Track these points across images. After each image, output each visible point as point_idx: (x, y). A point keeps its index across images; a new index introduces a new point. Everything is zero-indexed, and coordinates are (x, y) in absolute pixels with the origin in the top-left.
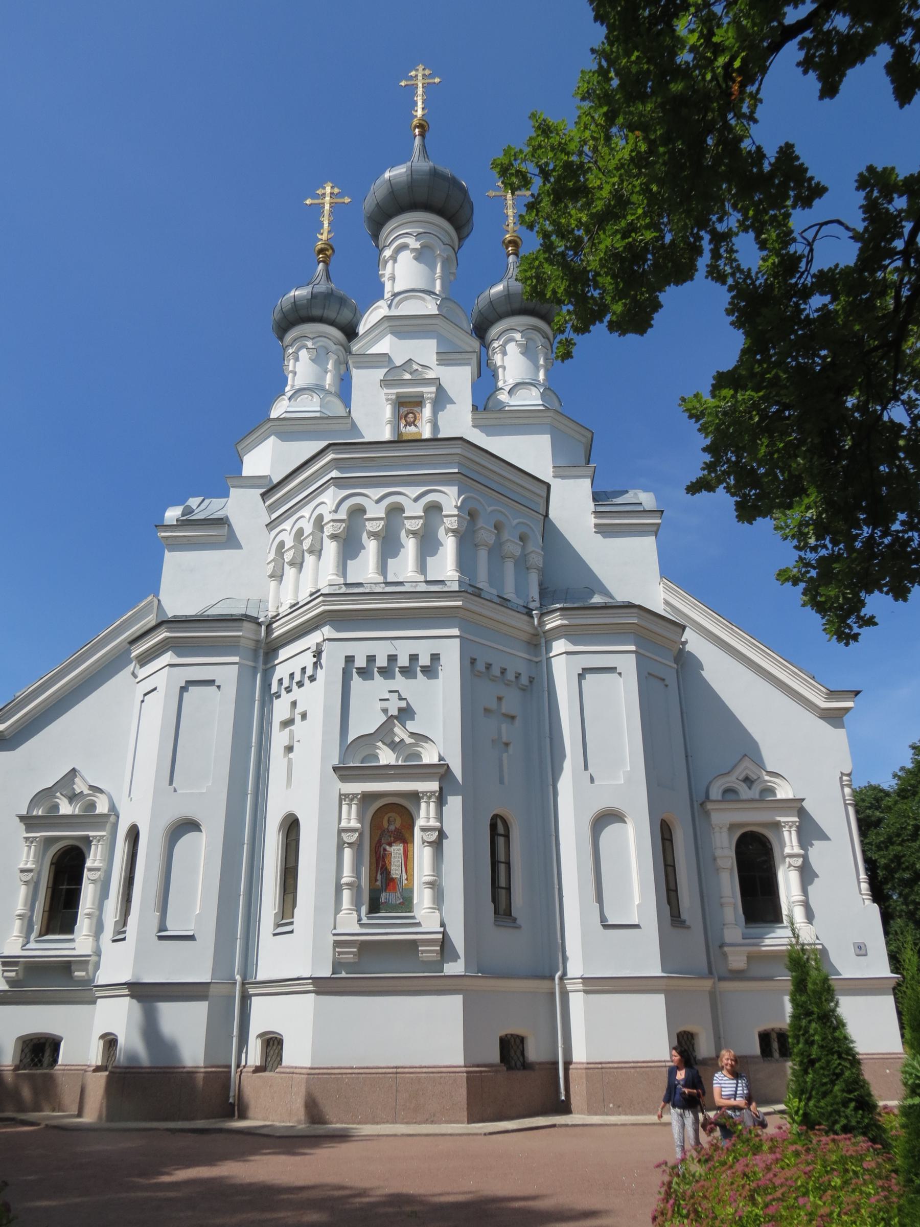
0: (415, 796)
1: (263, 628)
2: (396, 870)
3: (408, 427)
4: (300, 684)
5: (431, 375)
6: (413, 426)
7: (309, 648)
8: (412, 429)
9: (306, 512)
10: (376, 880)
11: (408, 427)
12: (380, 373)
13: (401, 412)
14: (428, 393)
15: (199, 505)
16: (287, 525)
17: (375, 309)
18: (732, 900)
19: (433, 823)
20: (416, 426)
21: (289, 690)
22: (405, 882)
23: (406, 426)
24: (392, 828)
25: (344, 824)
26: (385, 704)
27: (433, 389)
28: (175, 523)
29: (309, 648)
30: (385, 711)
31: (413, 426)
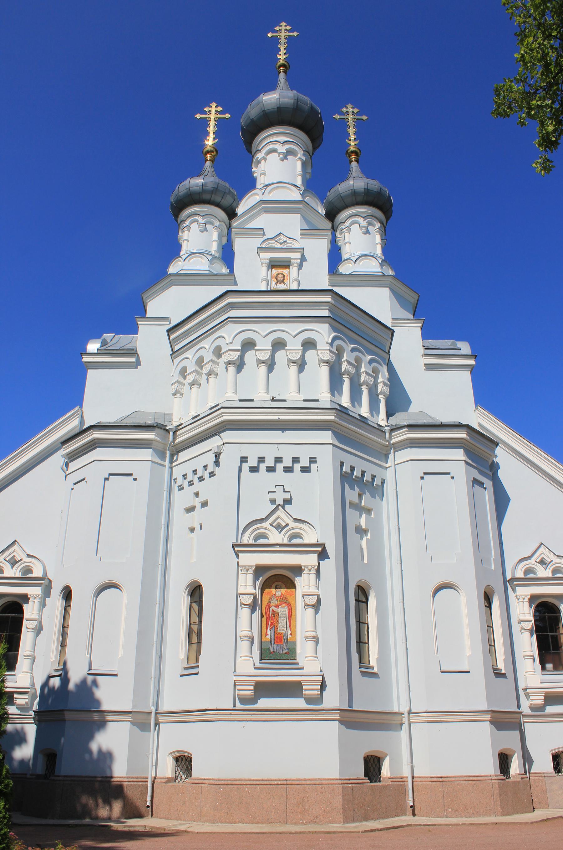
0: (298, 570)
1: (171, 433)
2: (282, 628)
3: (278, 284)
4: (201, 479)
5: (297, 245)
6: (282, 284)
7: (211, 450)
9: (207, 344)
10: (267, 635)
11: (278, 284)
12: (257, 242)
13: (273, 273)
15: (112, 340)
16: (189, 354)
17: (252, 195)
19: (313, 590)
20: (284, 283)
21: (191, 483)
22: (289, 636)
23: (276, 283)
25: (241, 590)
26: (272, 496)
27: (298, 255)
28: (96, 352)
29: (211, 450)
30: (273, 501)
31: (282, 284)
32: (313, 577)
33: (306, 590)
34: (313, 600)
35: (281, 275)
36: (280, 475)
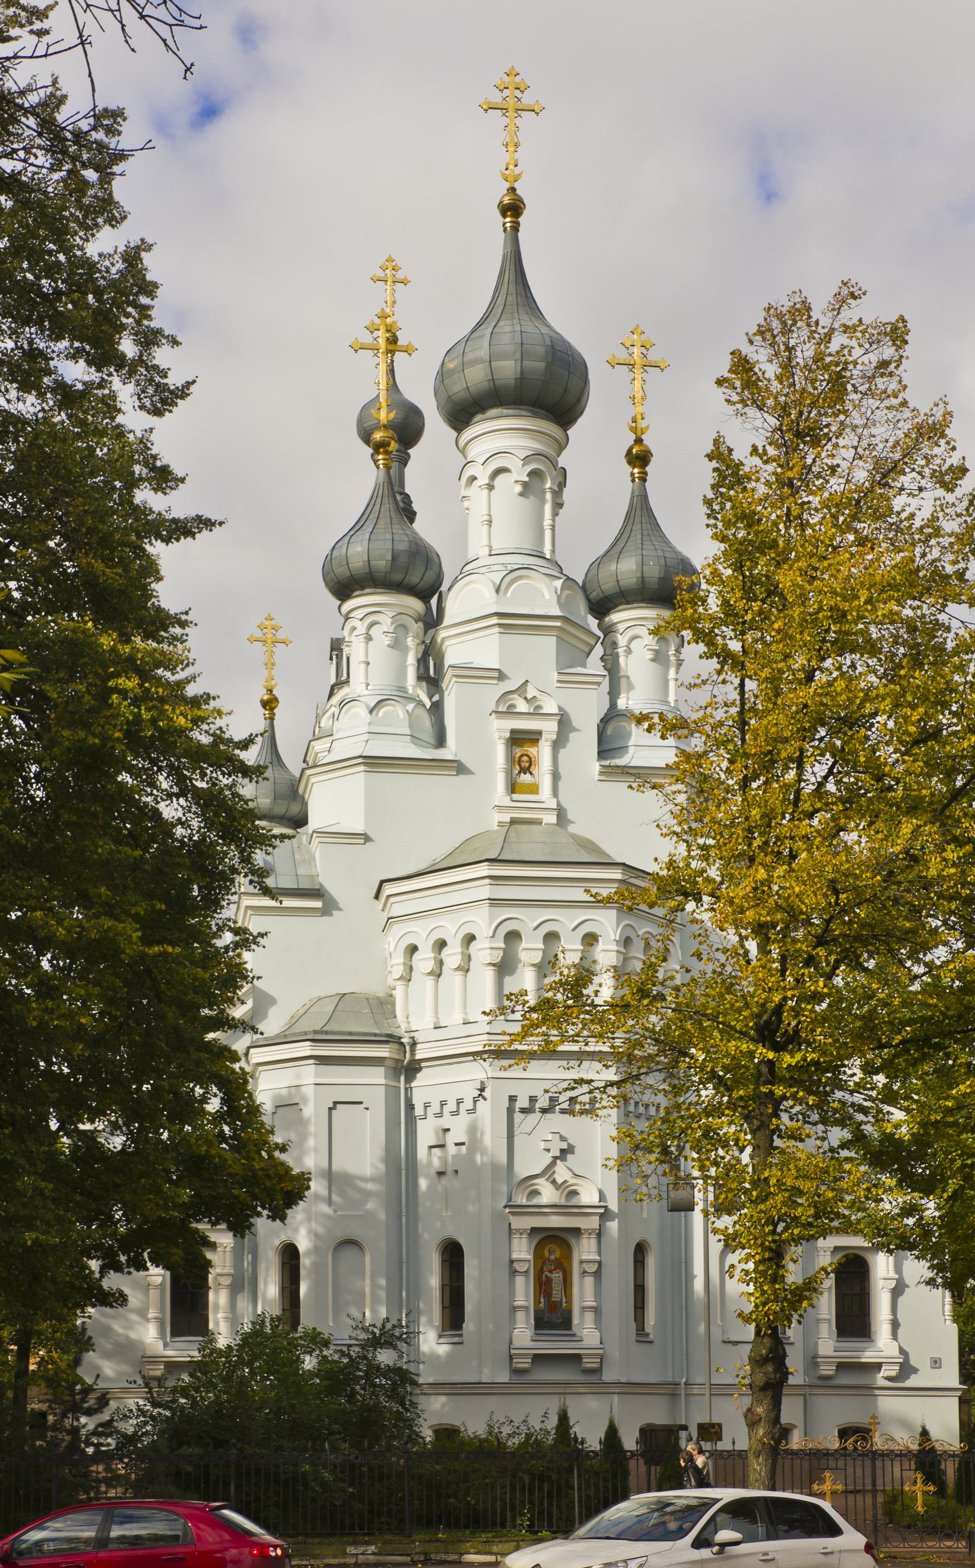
0: (577, 1232)
1: (408, 1048)
2: (557, 1294)
8: (525, 778)
14: (550, 732)
18: (827, 1317)
24: (552, 1257)
26: (548, 1145)
32: (593, 1242)
33: (584, 1257)
34: (594, 1268)
35: (525, 758)
36: (557, 1121)
